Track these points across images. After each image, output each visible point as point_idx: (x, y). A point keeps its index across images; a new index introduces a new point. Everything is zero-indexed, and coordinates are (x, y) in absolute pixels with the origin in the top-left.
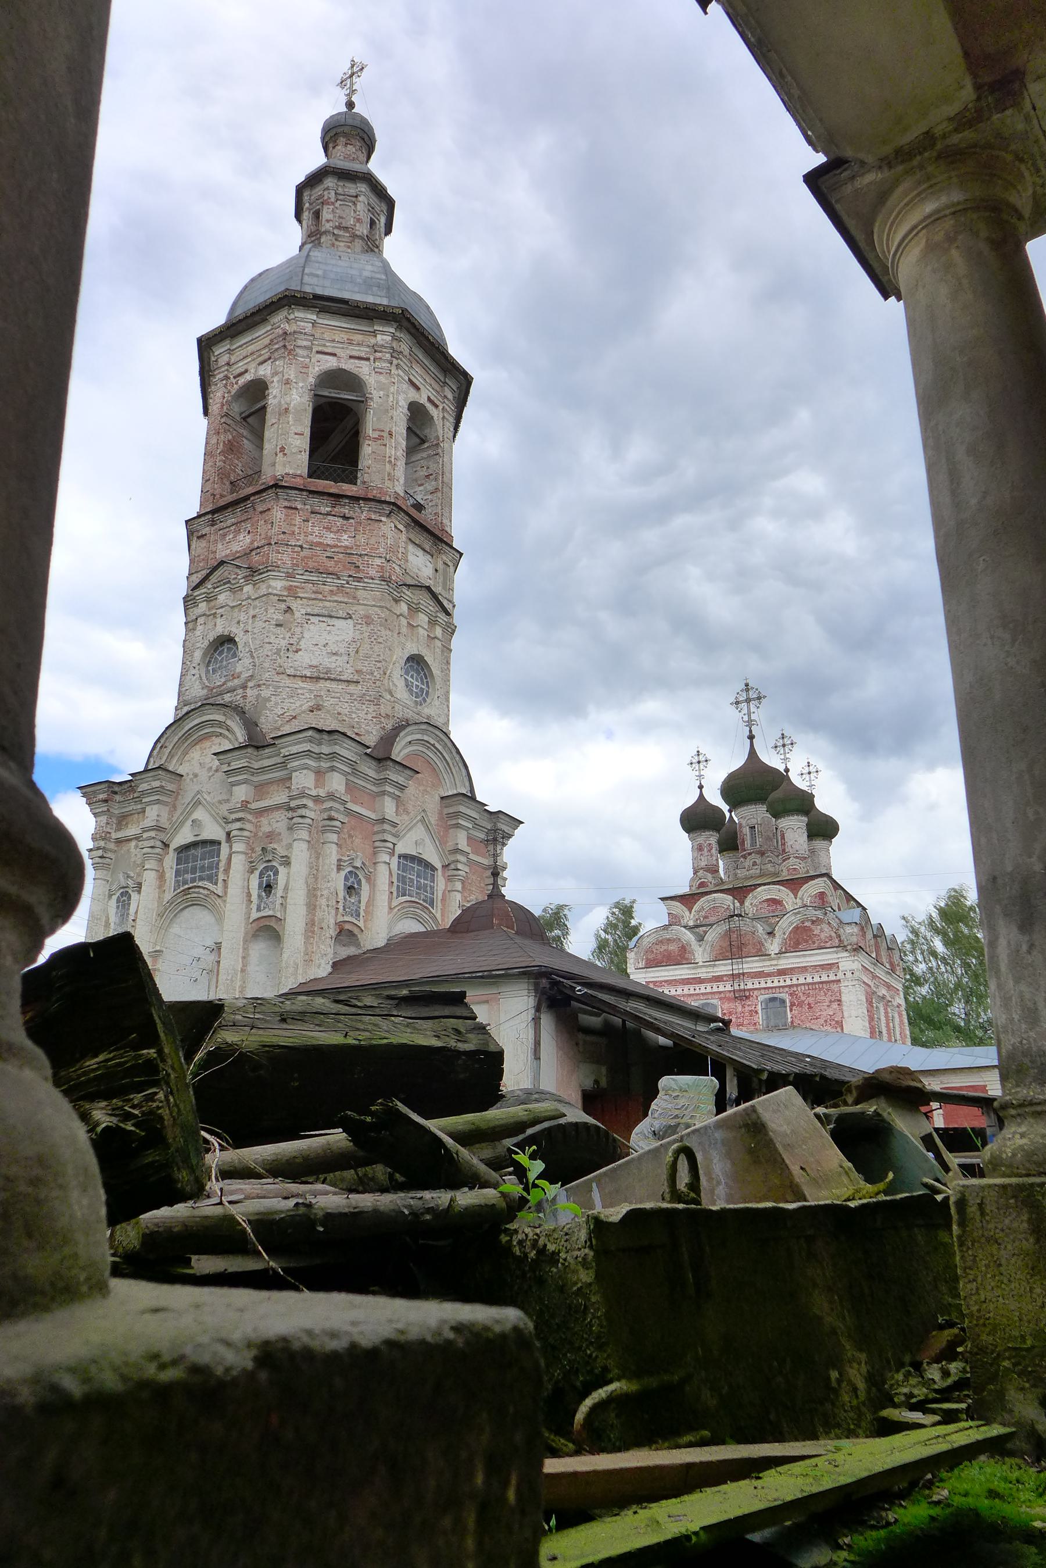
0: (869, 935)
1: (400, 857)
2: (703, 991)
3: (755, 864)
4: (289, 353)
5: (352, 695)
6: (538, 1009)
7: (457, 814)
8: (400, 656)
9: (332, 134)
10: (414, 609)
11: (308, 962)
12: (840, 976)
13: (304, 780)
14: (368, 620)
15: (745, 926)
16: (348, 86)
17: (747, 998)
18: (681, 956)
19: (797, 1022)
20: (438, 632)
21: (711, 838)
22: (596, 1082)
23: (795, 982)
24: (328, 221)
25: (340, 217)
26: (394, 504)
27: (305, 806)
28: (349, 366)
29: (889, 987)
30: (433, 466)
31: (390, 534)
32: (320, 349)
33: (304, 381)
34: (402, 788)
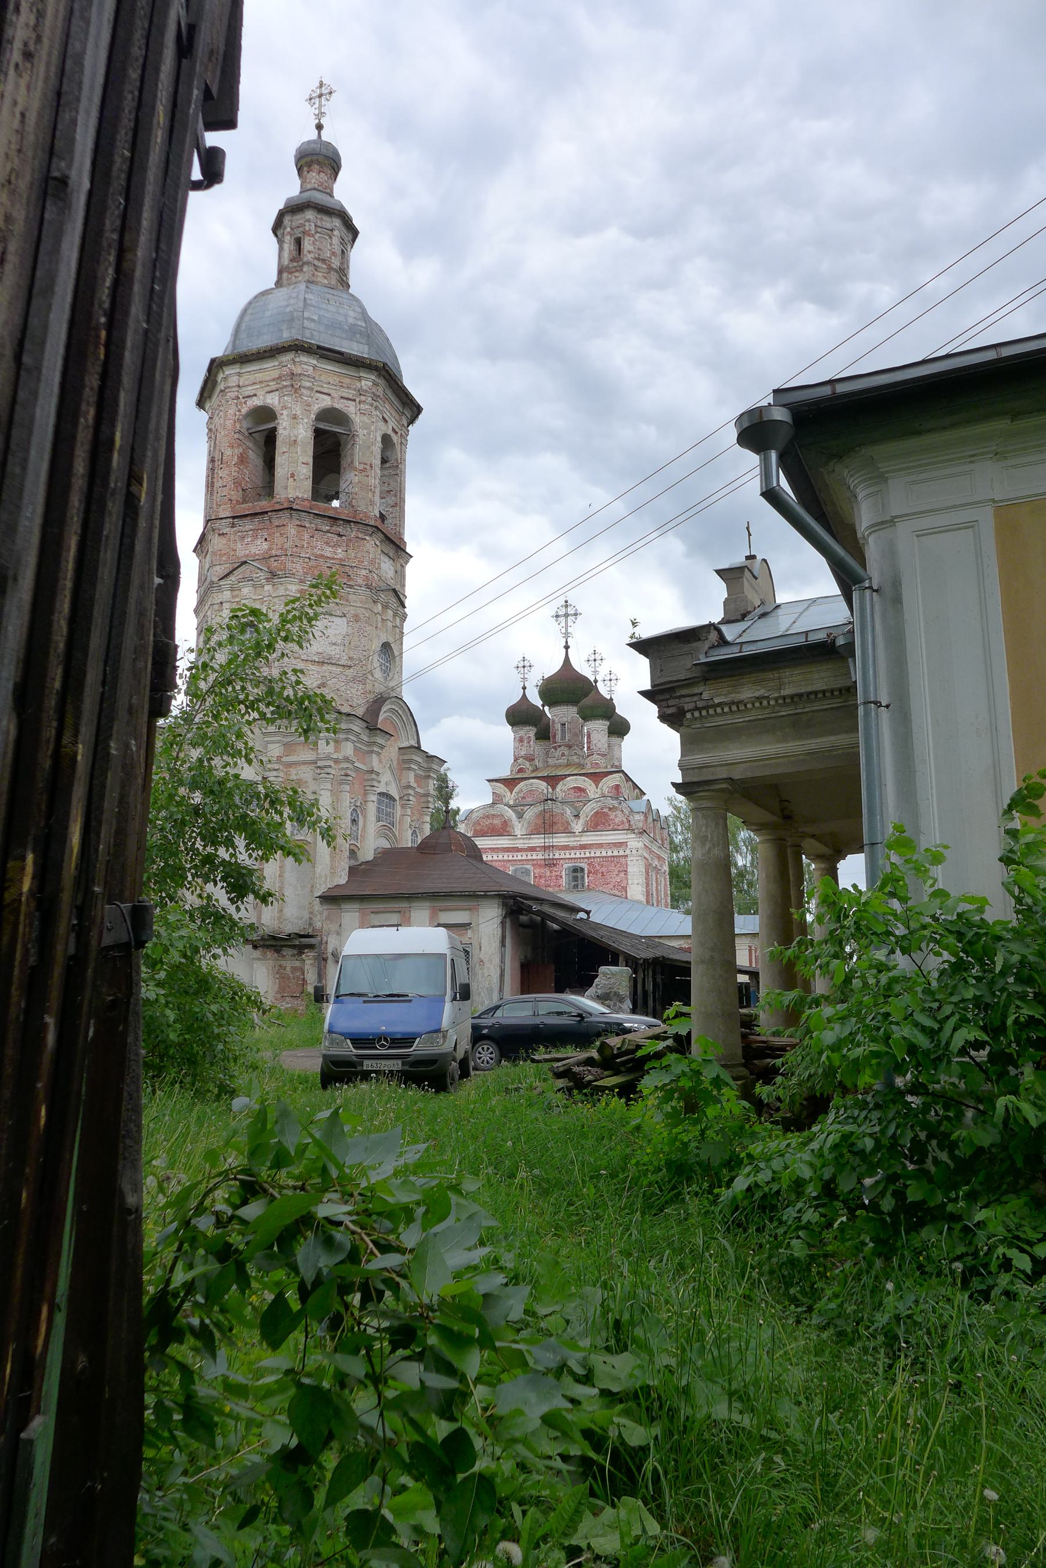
0: (650, 820)
2: (520, 858)
3: (563, 755)
4: (296, 392)
5: (347, 676)
6: (505, 917)
7: (410, 761)
8: (376, 645)
9: (308, 159)
10: (385, 607)
11: (333, 874)
12: (628, 852)
14: (357, 618)
15: (557, 808)
17: (555, 865)
18: (503, 829)
19: (592, 886)
21: (531, 732)
22: (526, 957)
23: (593, 855)
24: (309, 252)
25: (319, 249)
26: (376, 527)
27: (330, 766)
28: (339, 405)
29: (659, 858)
30: (393, 484)
31: (372, 550)
32: (319, 389)
33: (308, 418)
34: (382, 747)
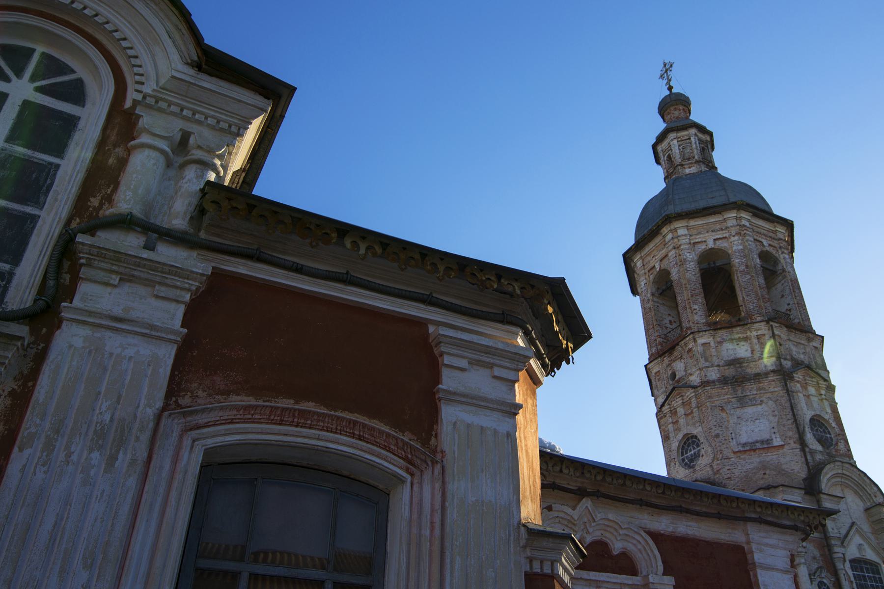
1: (851, 561)
16: (666, 77)
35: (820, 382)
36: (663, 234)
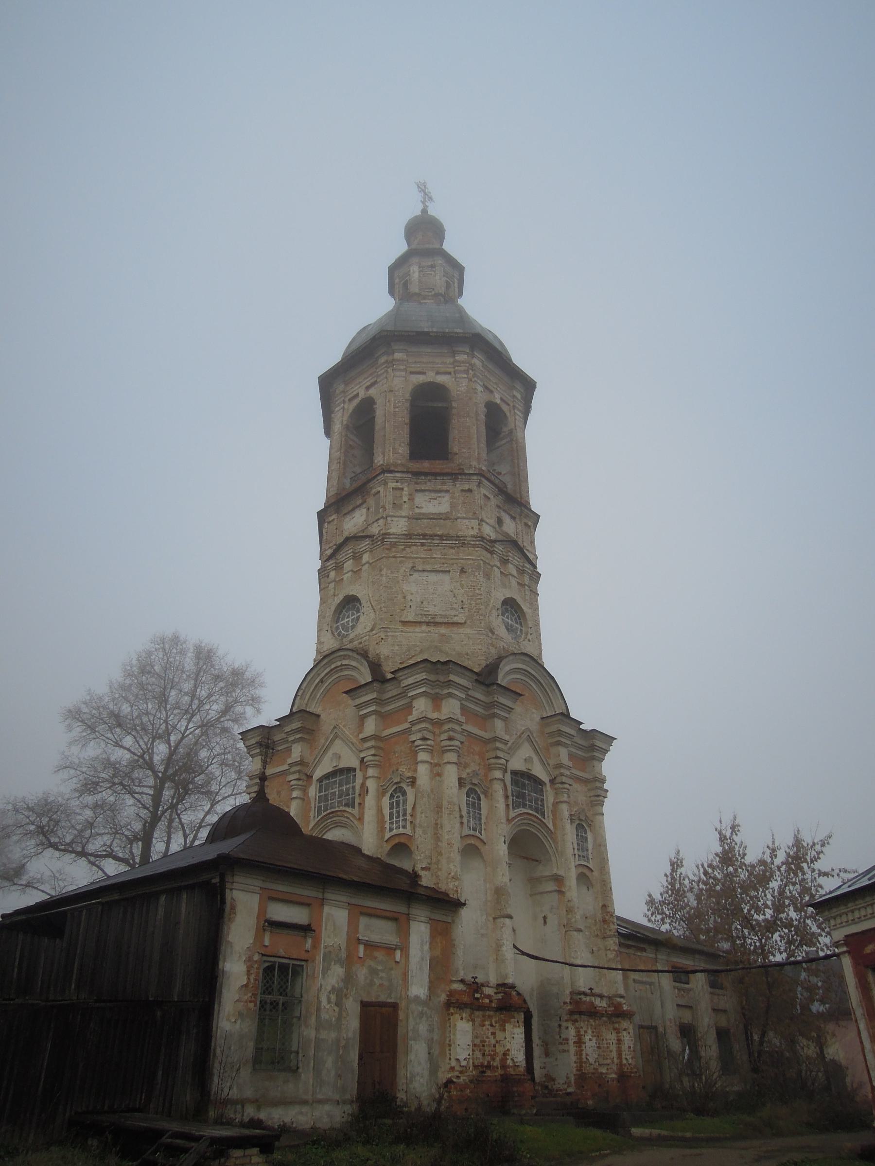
1: (511, 773)
10: (505, 562)
13: (421, 707)
20: (526, 580)
35: (525, 565)
36: (376, 356)
